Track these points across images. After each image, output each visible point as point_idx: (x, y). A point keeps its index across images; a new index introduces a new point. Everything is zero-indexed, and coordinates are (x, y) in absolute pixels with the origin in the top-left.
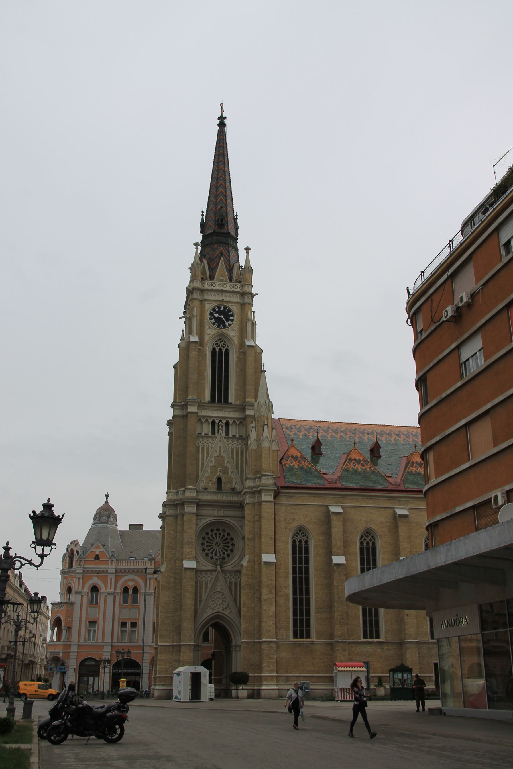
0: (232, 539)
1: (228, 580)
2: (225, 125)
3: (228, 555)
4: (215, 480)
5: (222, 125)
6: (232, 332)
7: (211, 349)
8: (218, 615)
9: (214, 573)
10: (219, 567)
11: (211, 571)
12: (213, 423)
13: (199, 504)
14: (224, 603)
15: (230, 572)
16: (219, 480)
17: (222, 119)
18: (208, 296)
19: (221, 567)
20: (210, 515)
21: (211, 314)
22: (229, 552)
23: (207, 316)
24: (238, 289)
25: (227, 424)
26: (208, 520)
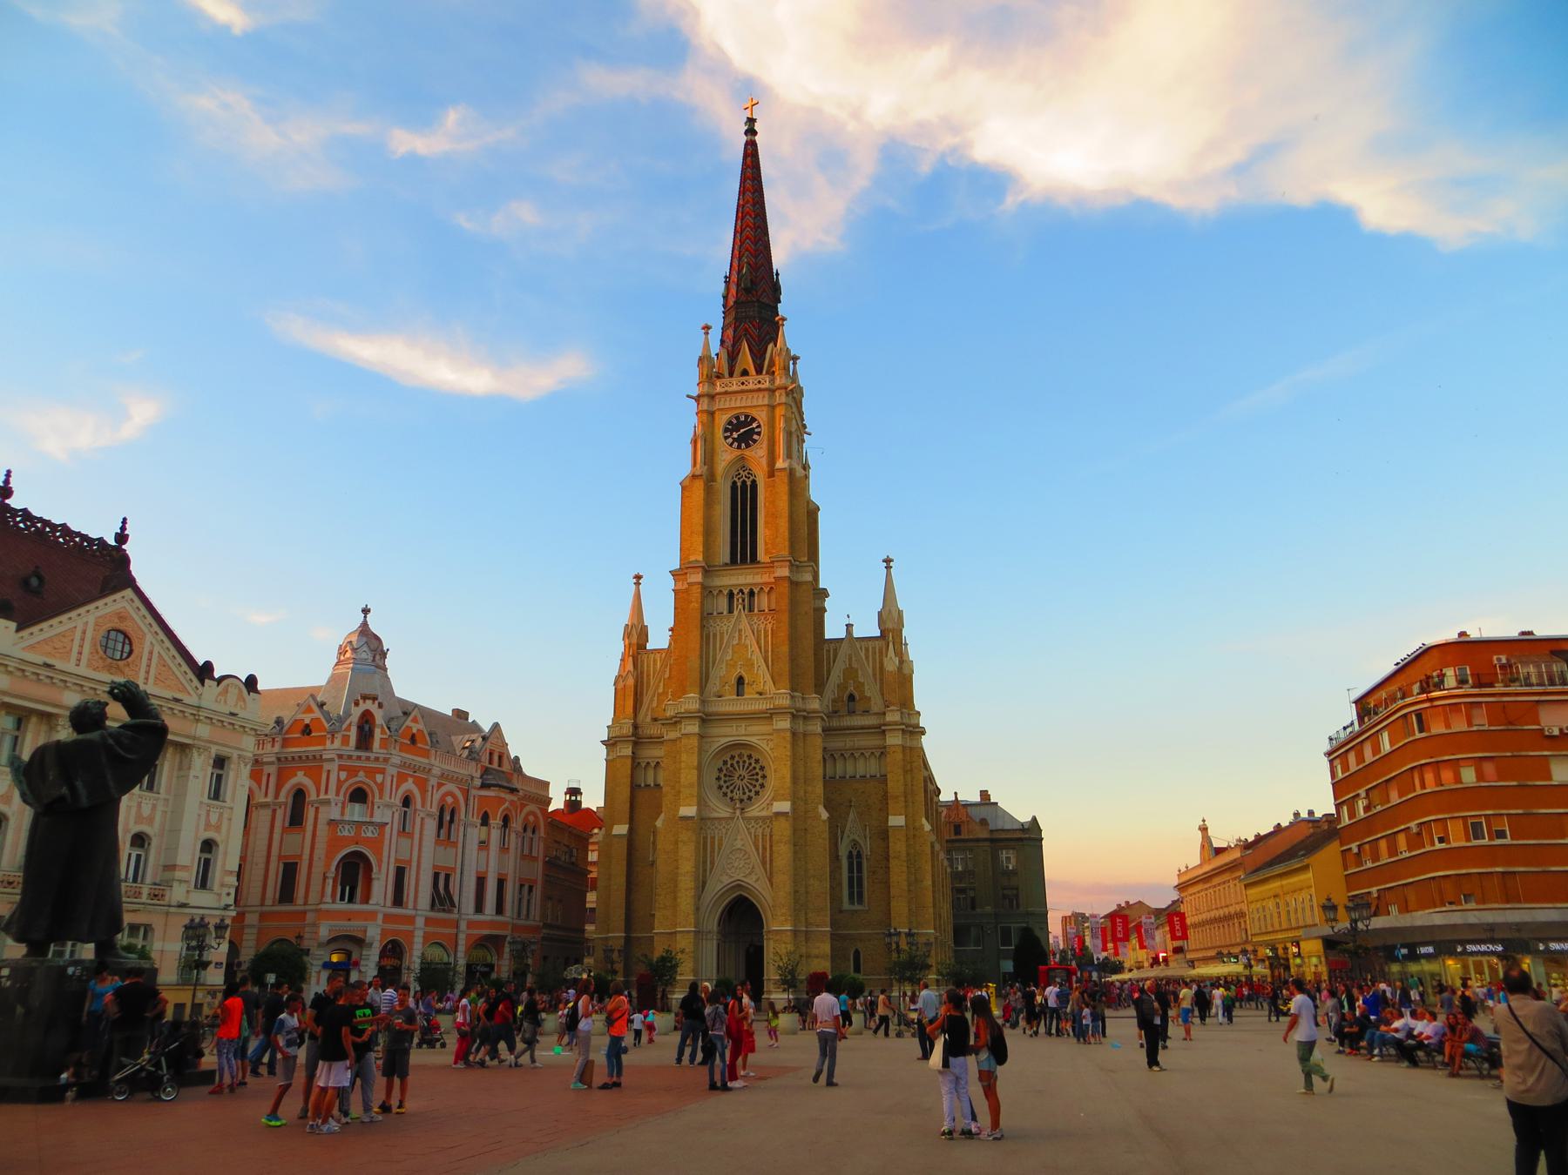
0: (762, 768)
2: (755, 133)
3: (757, 793)
4: (733, 681)
5: (751, 131)
6: (757, 455)
7: (729, 484)
12: (731, 595)
13: (706, 719)
15: (756, 819)
16: (740, 681)
17: (751, 121)
18: (721, 403)
20: (725, 735)
21: (726, 430)
23: (719, 434)
24: (767, 385)
25: (752, 593)
26: (724, 740)
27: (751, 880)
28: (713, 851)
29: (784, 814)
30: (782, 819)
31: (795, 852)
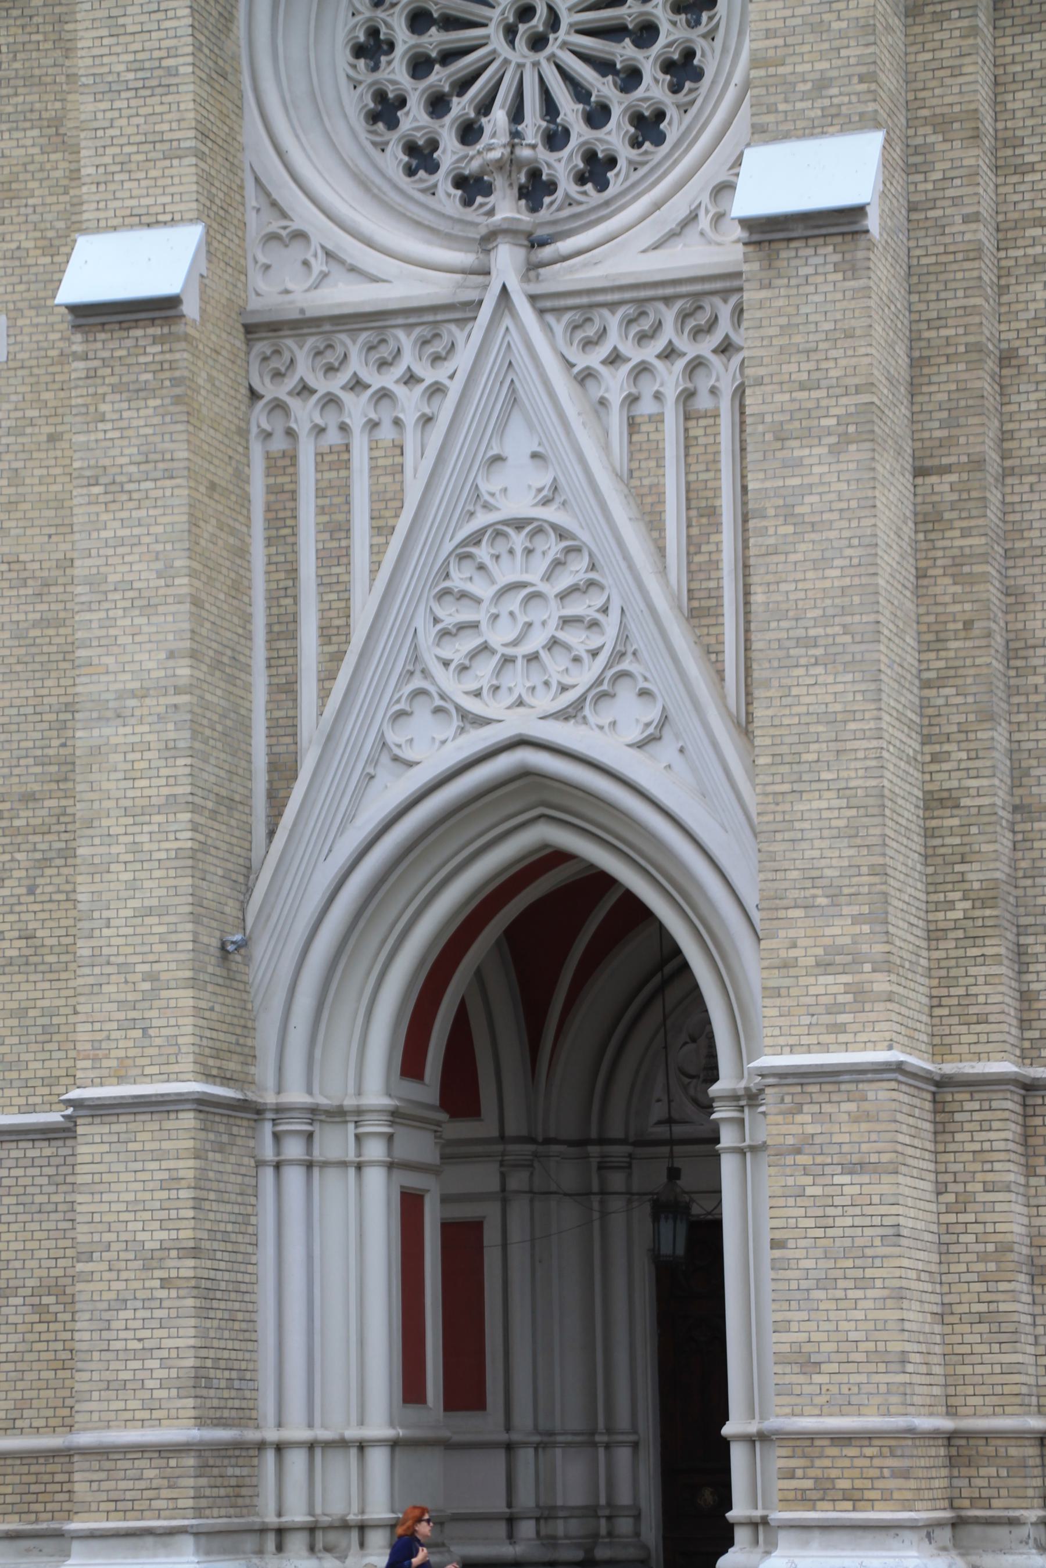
1: (615, 384)
3: (648, 127)
8: (525, 774)
9: (460, 335)
10: (507, 259)
11: (434, 321)
14: (577, 639)
15: (639, 300)
19: (532, 268)
22: (654, 87)
27: (609, 737)
28: (335, 556)
29: (841, 223)
30: (814, 262)
31: (928, 520)
